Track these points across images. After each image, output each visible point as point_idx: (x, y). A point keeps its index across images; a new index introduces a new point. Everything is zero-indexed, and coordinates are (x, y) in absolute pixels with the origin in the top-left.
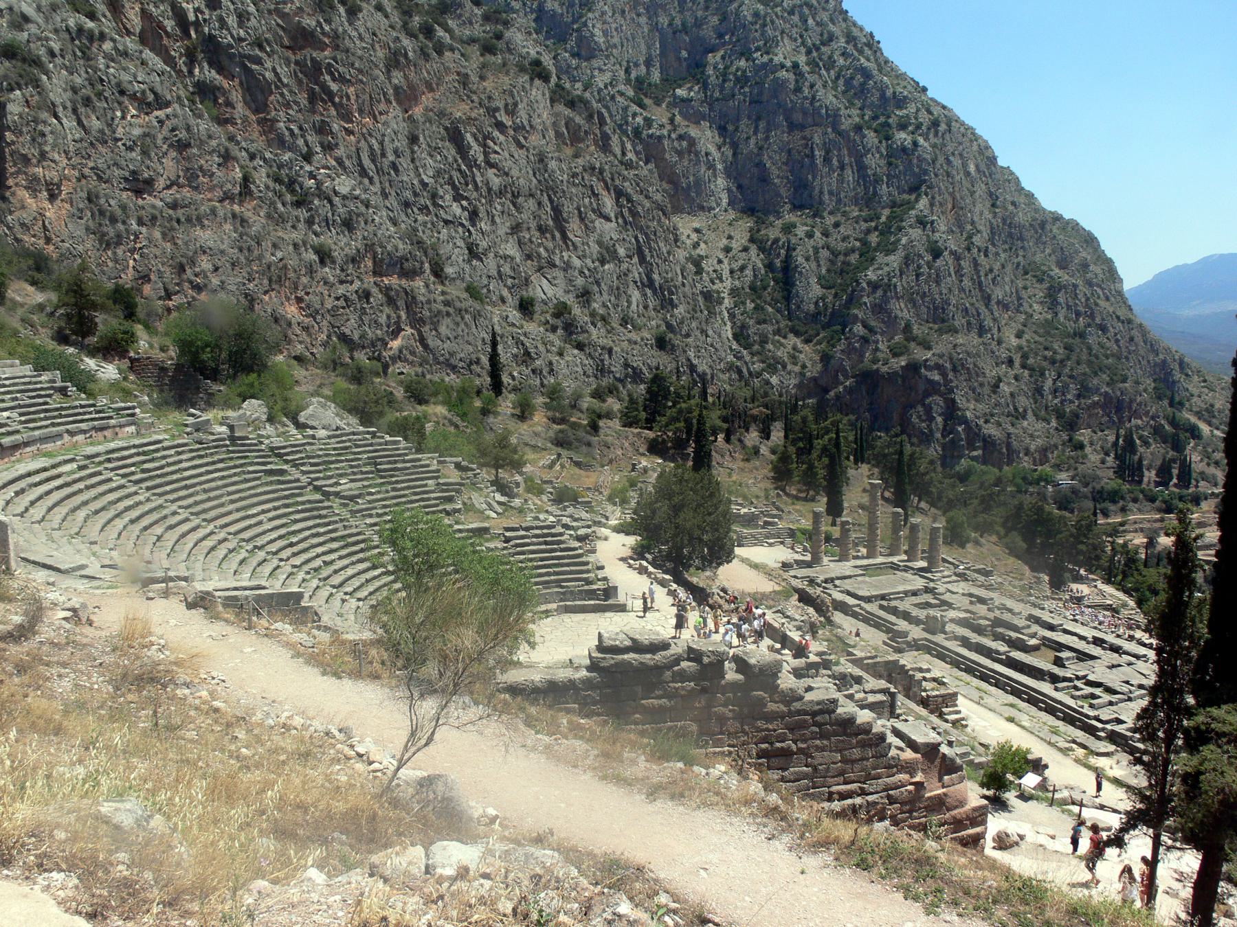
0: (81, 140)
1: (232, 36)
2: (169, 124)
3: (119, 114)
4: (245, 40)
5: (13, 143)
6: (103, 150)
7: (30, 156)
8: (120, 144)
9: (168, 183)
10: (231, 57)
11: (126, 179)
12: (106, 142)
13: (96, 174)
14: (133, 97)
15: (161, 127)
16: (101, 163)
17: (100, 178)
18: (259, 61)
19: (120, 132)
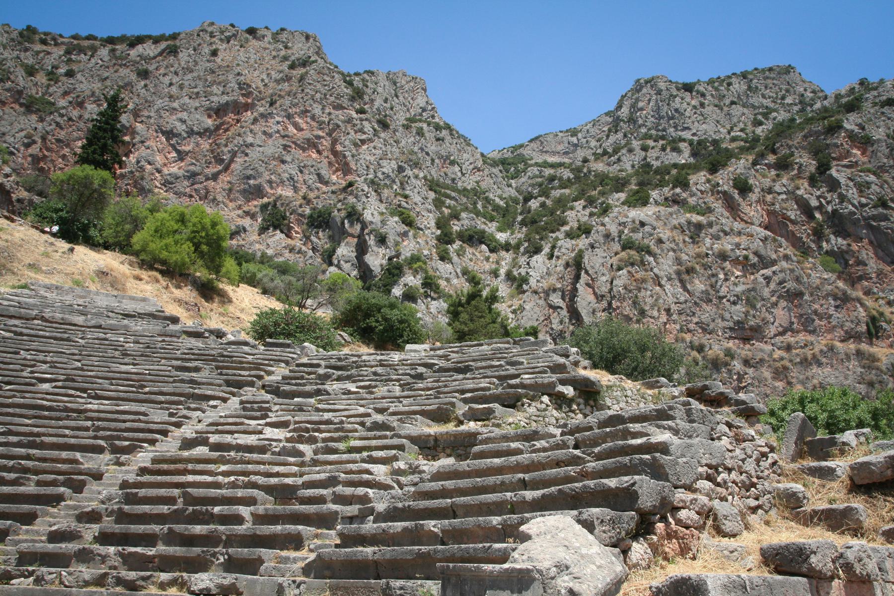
0: (686, 301)
1: (853, 205)
2: (776, 278)
3: (722, 276)
4: (867, 205)
5: (618, 308)
6: (708, 308)
7: (631, 316)
8: (725, 300)
9: (780, 329)
10: (856, 223)
11: (731, 329)
12: (711, 301)
13: (700, 327)
14: (736, 262)
15: (768, 283)
16: (705, 318)
17: (704, 330)
18: (886, 218)
19: (723, 291)
